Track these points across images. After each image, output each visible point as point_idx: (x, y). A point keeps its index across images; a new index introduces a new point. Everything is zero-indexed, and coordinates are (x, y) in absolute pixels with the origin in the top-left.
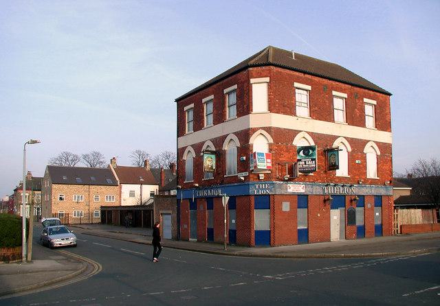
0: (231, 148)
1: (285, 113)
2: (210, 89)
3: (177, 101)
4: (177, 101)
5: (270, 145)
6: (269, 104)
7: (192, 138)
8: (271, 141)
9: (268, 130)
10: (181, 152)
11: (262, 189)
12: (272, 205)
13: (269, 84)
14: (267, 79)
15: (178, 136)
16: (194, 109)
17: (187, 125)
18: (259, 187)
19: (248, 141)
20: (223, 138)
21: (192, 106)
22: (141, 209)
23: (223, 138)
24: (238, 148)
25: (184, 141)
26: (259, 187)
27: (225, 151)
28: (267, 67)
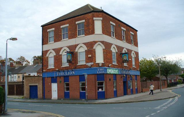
0: (81, 50)
1: (108, 35)
2: (67, 21)
3: (42, 26)
4: (42, 26)
5: (103, 49)
6: (102, 30)
7: (52, 45)
8: (104, 48)
9: (103, 42)
10: (44, 53)
11: (102, 71)
12: (105, 79)
13: (103, 21)
14: (101, 19)
15: (43, 44)
16: (55, 31)
17: (49, 39)
18: (99, 70)
19: (92, 47)
20: (76, 46)
21: (52, 30)
22: (14, 84)
23: (76, 46)
24: (86, 51)
25: (46, 47)
26: (99, 70)
27: (77, 52)
28: (101, 13)
